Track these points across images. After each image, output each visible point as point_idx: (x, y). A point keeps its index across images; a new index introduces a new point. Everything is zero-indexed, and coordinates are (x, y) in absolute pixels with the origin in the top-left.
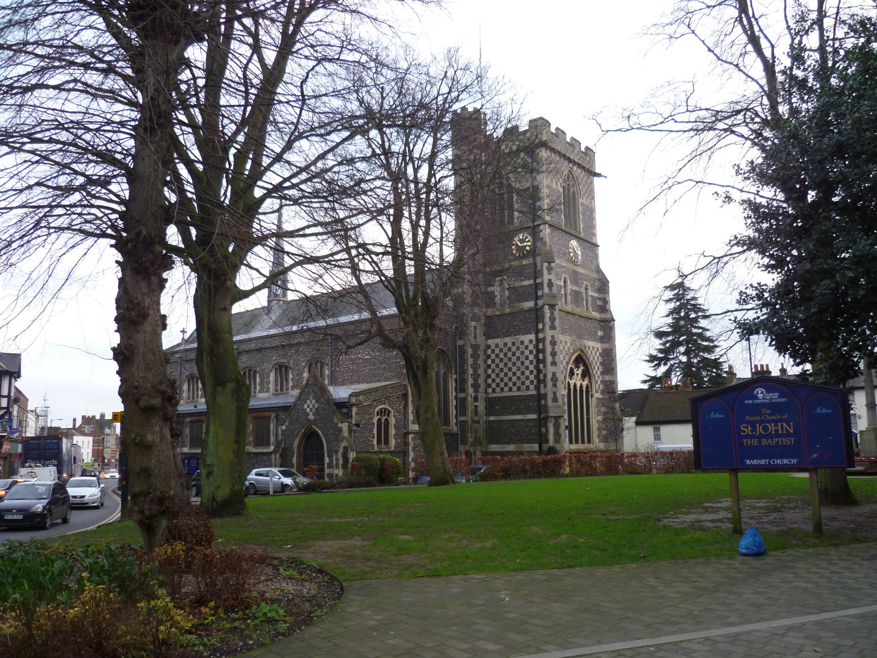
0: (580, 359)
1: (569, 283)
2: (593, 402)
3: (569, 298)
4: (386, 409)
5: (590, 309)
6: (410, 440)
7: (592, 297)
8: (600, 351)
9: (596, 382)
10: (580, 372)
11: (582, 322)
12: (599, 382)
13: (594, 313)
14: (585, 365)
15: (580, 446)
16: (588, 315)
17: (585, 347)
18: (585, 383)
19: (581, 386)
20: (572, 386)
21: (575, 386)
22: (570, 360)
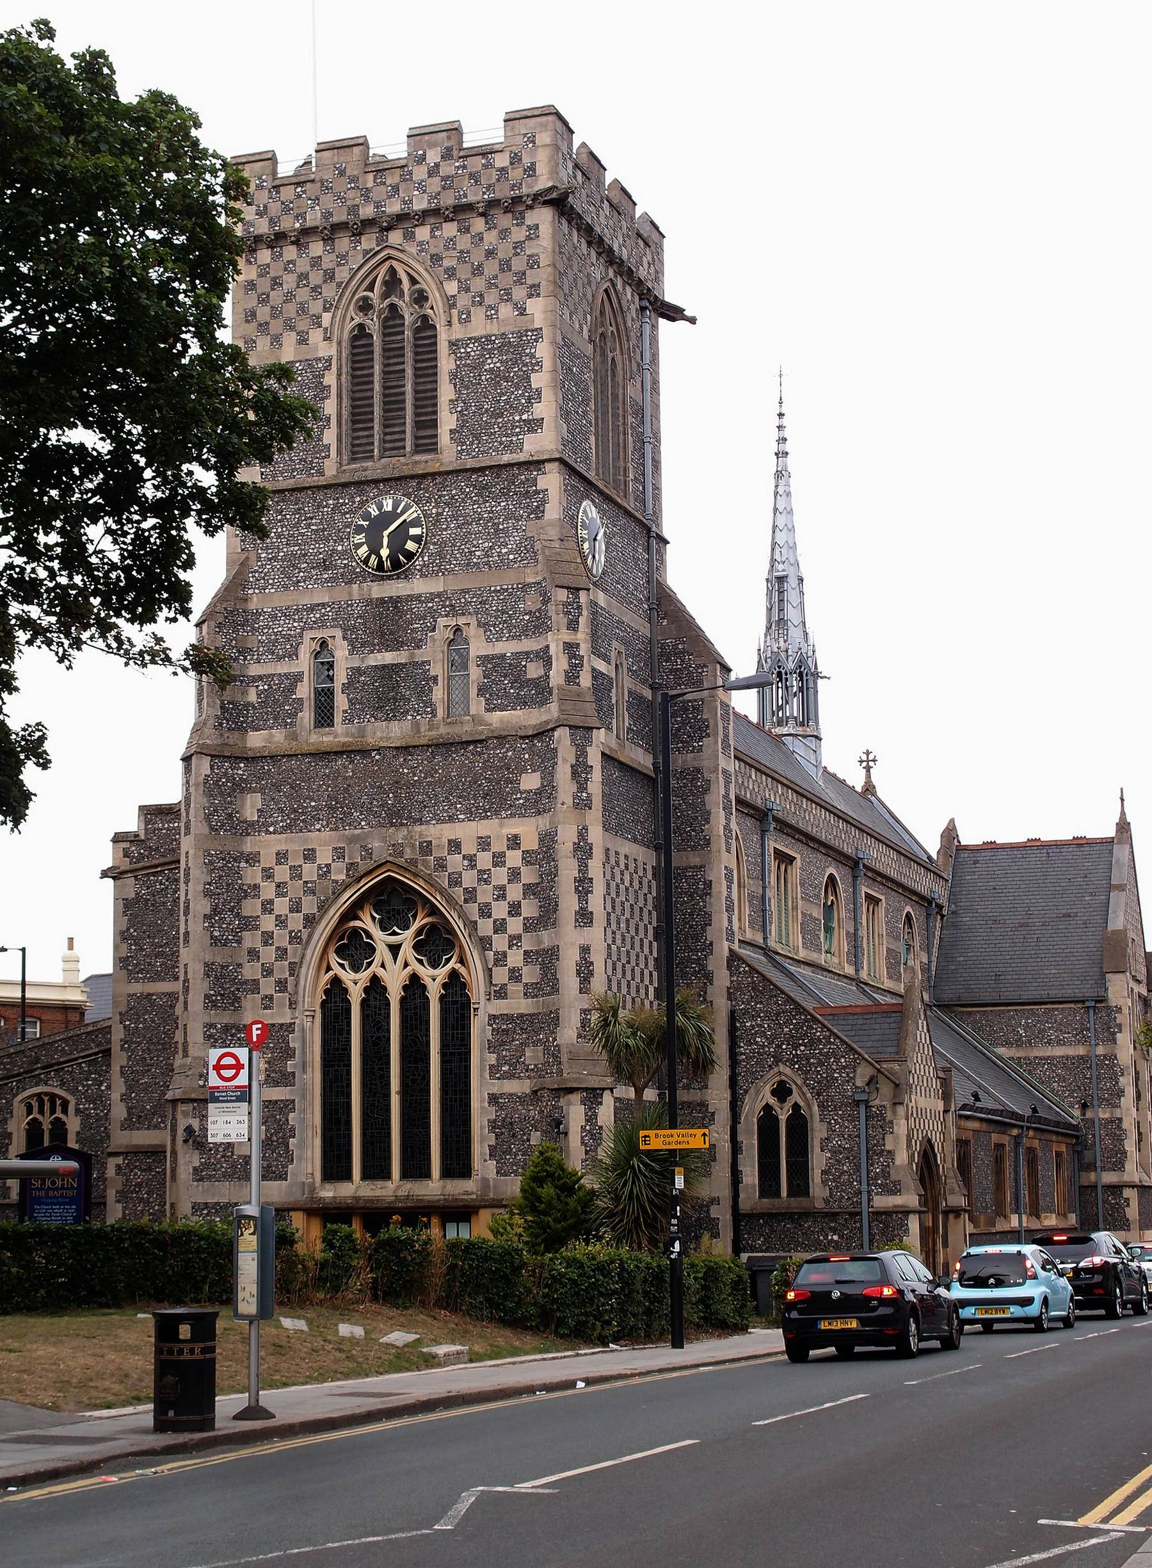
0: (393, 900)
1: (341, 652)
2: (479, 1030)
3: (341, 702)
4: (53, 1097)
5: (477, 706)
6: (111, 1172)
7: (484, 660)
8: (530, 842)
9: (501, 959)
10: (407, 937)
11: (411, 769)
12: (515, 958)
13: (497, 718)
14: (433, 911)
15: (393, 1188)
16: (465, 730)
17: (426, 848)
18: (434, 979)
19: (415, 985)
20: (356, 995)
21: (376, 987)
22: (323, 908)
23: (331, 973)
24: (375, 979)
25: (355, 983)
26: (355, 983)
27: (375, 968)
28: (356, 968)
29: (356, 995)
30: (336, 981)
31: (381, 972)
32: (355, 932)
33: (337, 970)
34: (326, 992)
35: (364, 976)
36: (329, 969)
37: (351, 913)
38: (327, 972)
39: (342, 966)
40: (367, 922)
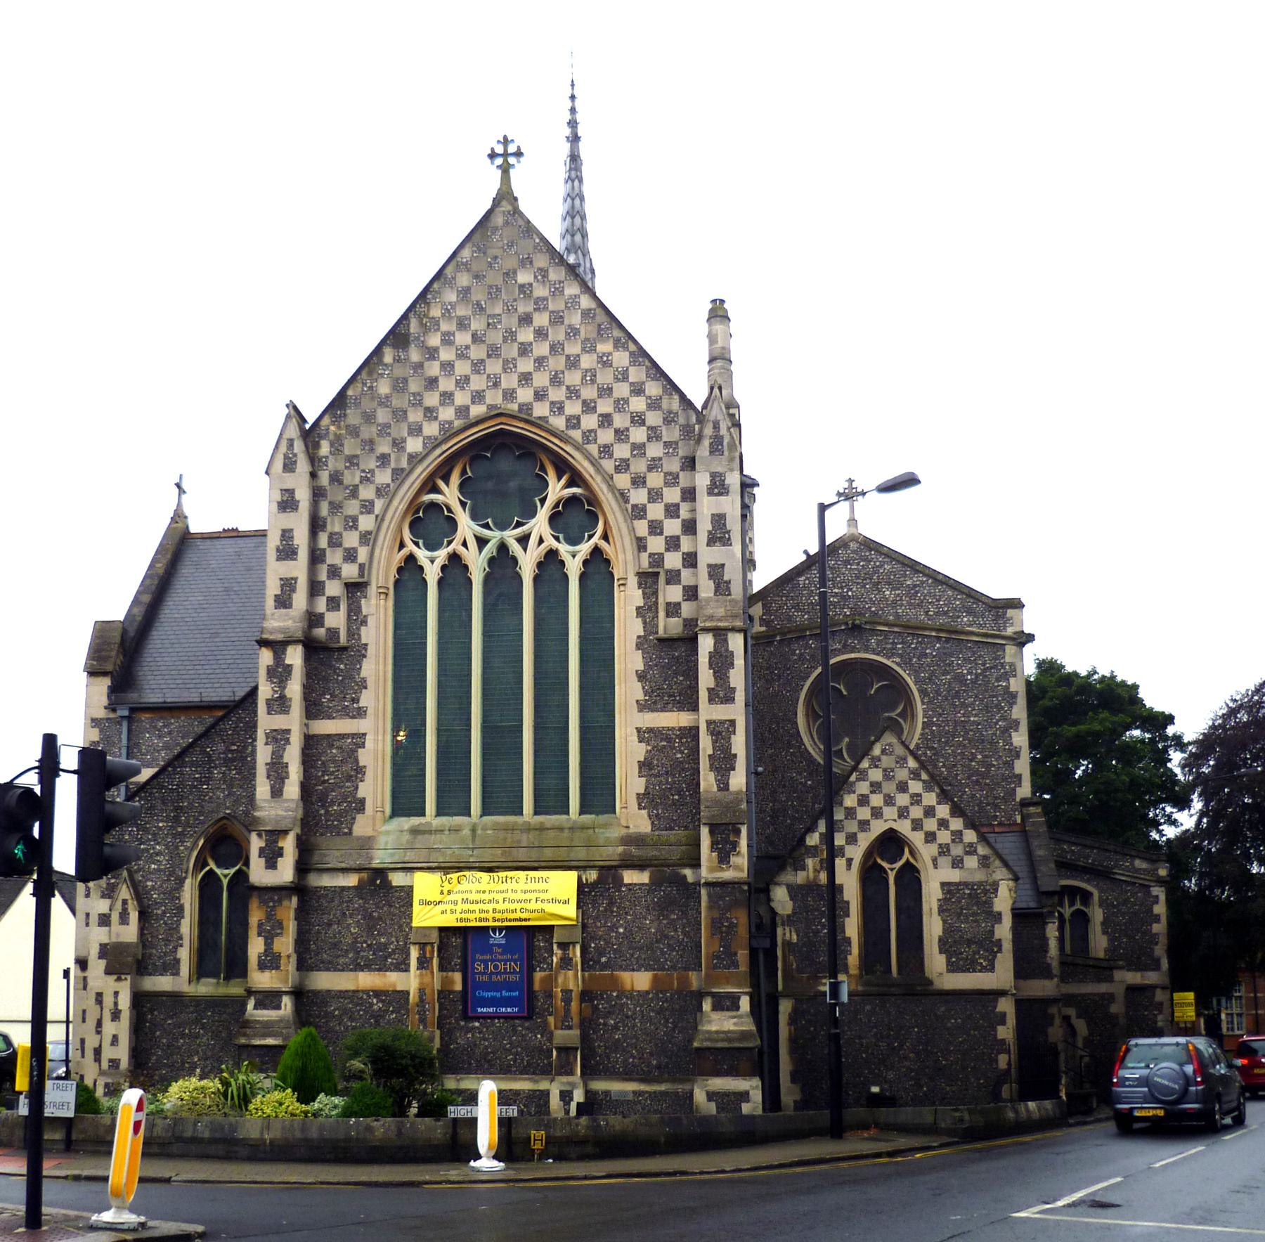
20: (432, 574)
23: (405, 552)
24: (454, 558)
25: (432, 564)
26: (432, 564)
27: (456, 546)
28: (431, 547)
29: (432, 574)
30: (411, 558)
31: (461, 550)
32: (434, 506)
33: (411, 547)
34: (400, 570)
35: (442, 555)
36: (402, 546)
37: (430, 486)
38: (400, 550)
39: (417, 544)
40: (450, 494)
